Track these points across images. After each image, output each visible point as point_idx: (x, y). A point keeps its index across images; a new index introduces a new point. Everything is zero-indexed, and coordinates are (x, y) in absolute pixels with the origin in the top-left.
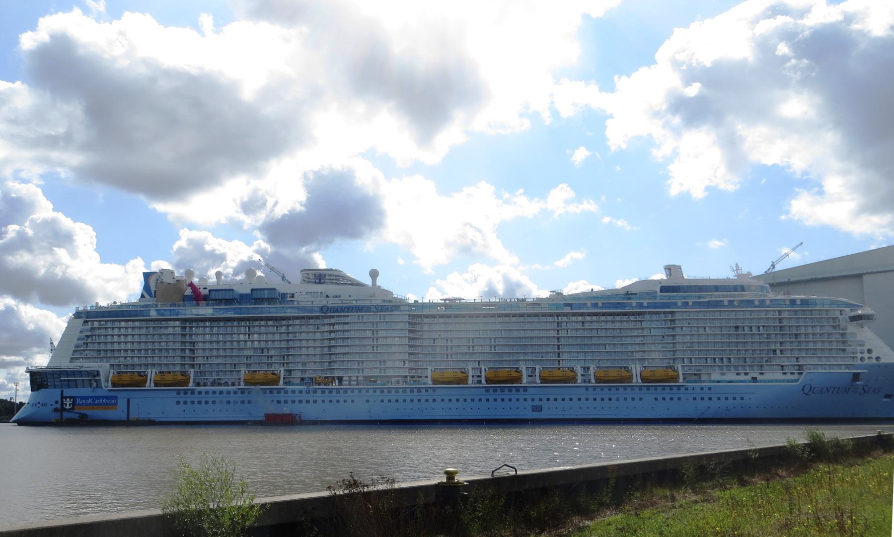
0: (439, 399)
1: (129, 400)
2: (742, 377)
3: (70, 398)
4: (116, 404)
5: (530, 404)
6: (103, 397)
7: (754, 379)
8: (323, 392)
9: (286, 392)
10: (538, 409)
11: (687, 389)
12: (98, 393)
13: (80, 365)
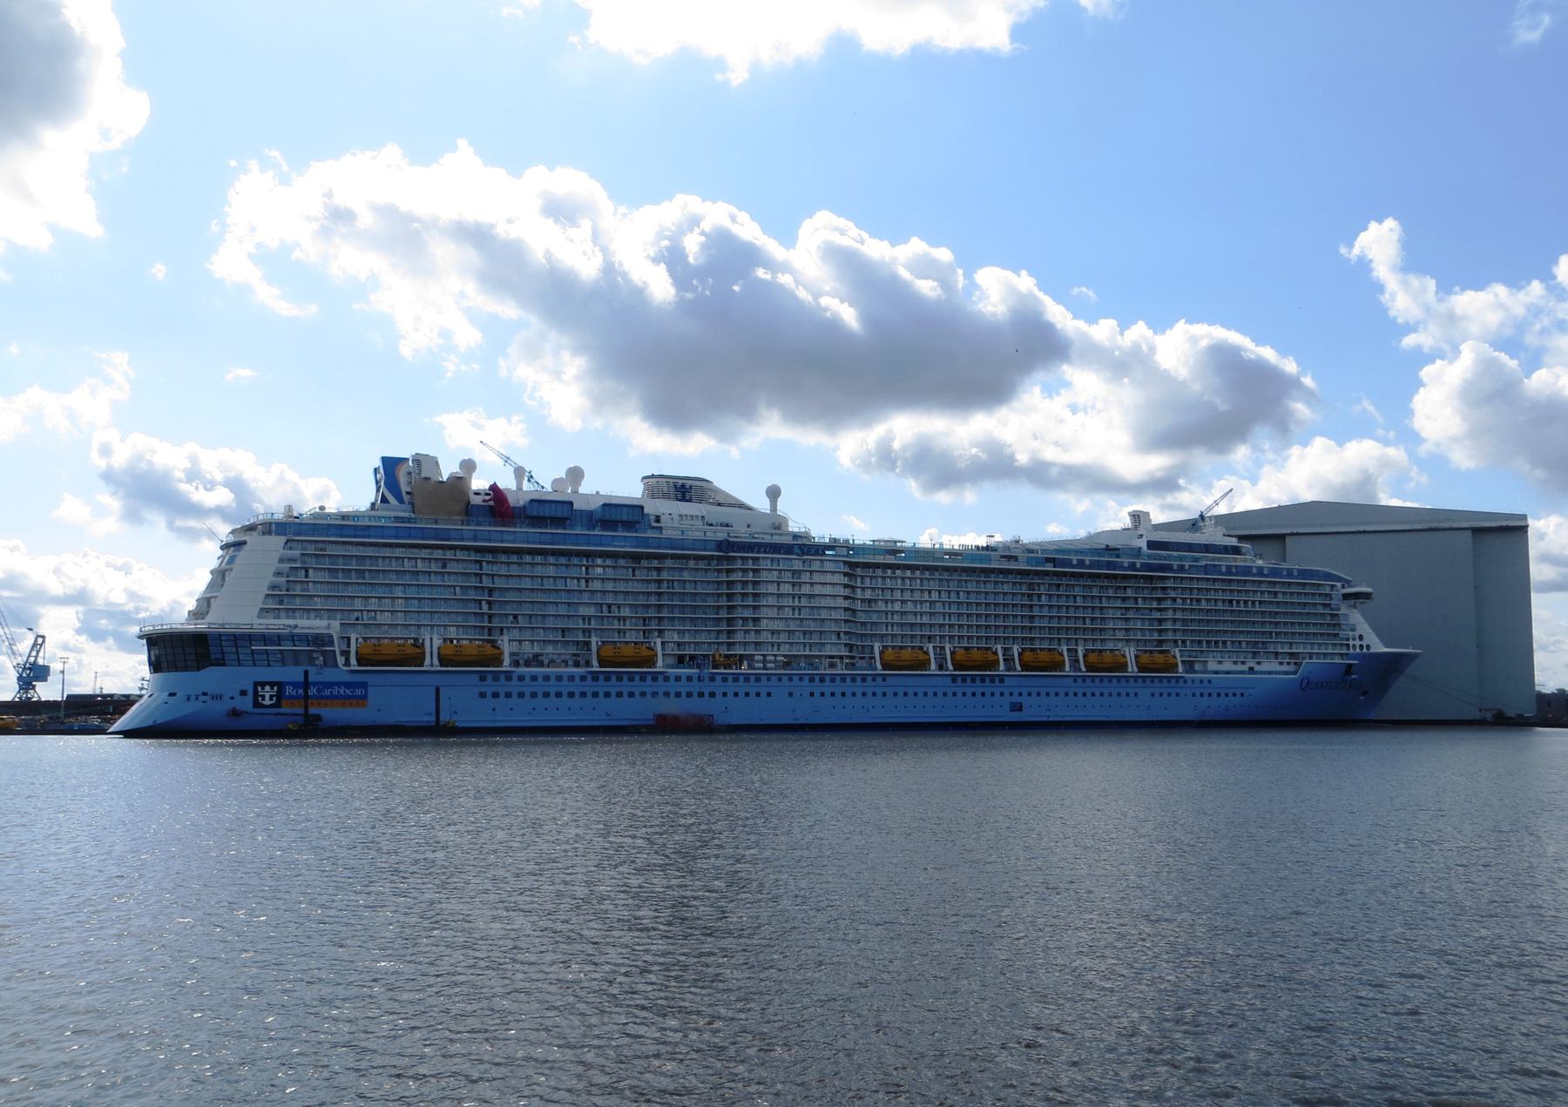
0: (890, 691)
1: (438, 690)
2: (1240, 667)
3: (272, 685)
4: (364, 697)
5: (1007, 700)
6: (339, 684)
7: (1251, 669)
8: (725, 680)
9: (667, 679)
10: (1017, 707)
12: (329, 675)
13: (292, 622)
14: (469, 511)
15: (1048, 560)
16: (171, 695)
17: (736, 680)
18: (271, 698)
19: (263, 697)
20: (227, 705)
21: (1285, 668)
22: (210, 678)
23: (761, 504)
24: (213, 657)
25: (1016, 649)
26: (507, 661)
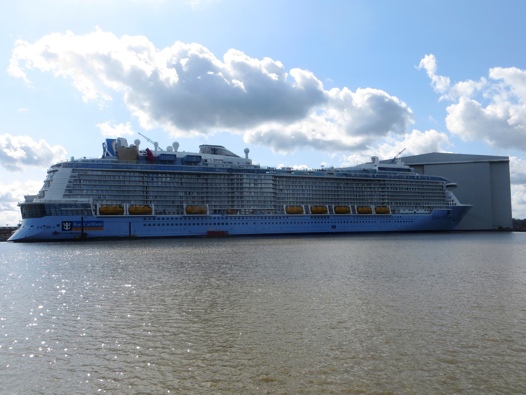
0: (289, 222)
1: (130, 223)
2: (411, 212)
3: (69, 222)
4: (103, 226)
6: (93, 222)
8: (231, 218)
10: (334, 227)
12: (89, 219)
13: (75, 199)
14: (138, 158)
15: (344, 174)
16: (31, 226)
17: (235, 218)
18: (68, 227)
19: (66, 227)
20: (52, 230)
21: (427, 212)
22: (45, 220)
23: (243, 155)
24: (47, 212)
25: (333, 206)
26: (153, 213)
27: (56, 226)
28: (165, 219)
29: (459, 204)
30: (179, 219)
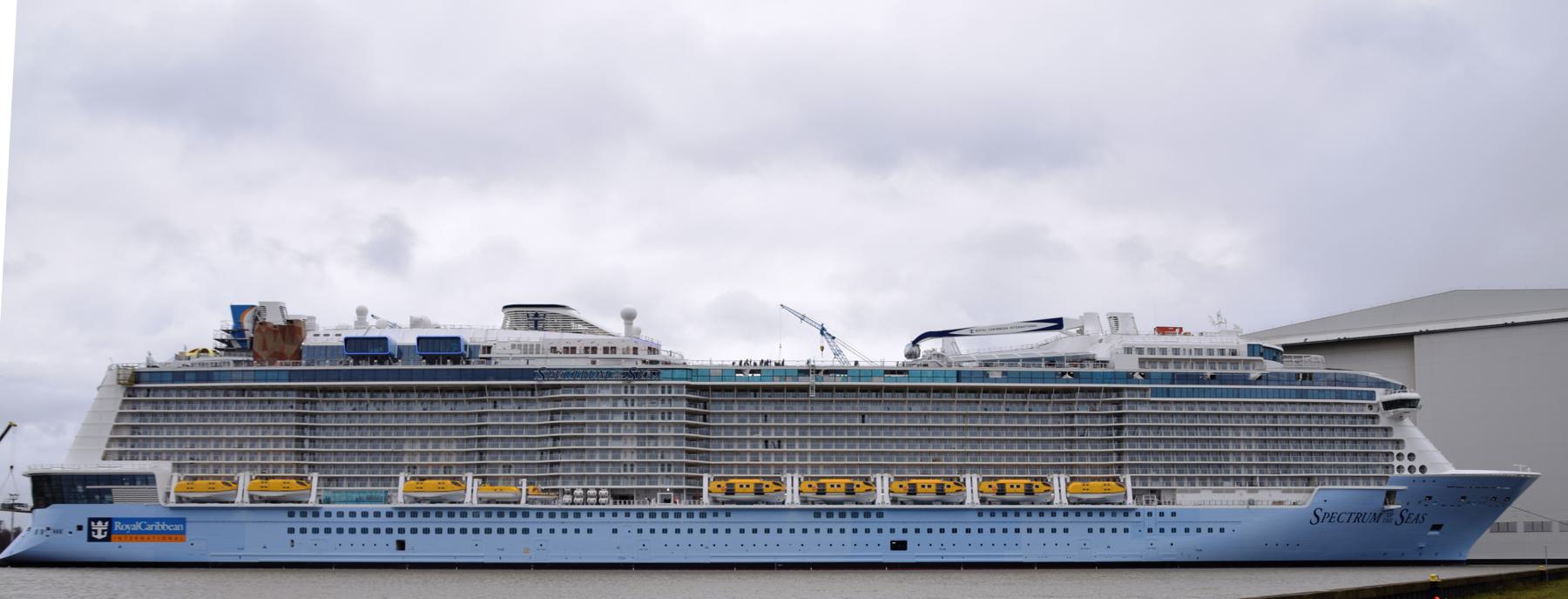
3: (104, 520)
4: (183, 533)
5: (887, 538)
6: (161, 520)
10: (900, 546)
11: (1138, 514)
17: (552, 515)
22: (53, 513)
27: (74, 529)
28: (359, 514)
29: (1443, 467)
30: (383, 514)
